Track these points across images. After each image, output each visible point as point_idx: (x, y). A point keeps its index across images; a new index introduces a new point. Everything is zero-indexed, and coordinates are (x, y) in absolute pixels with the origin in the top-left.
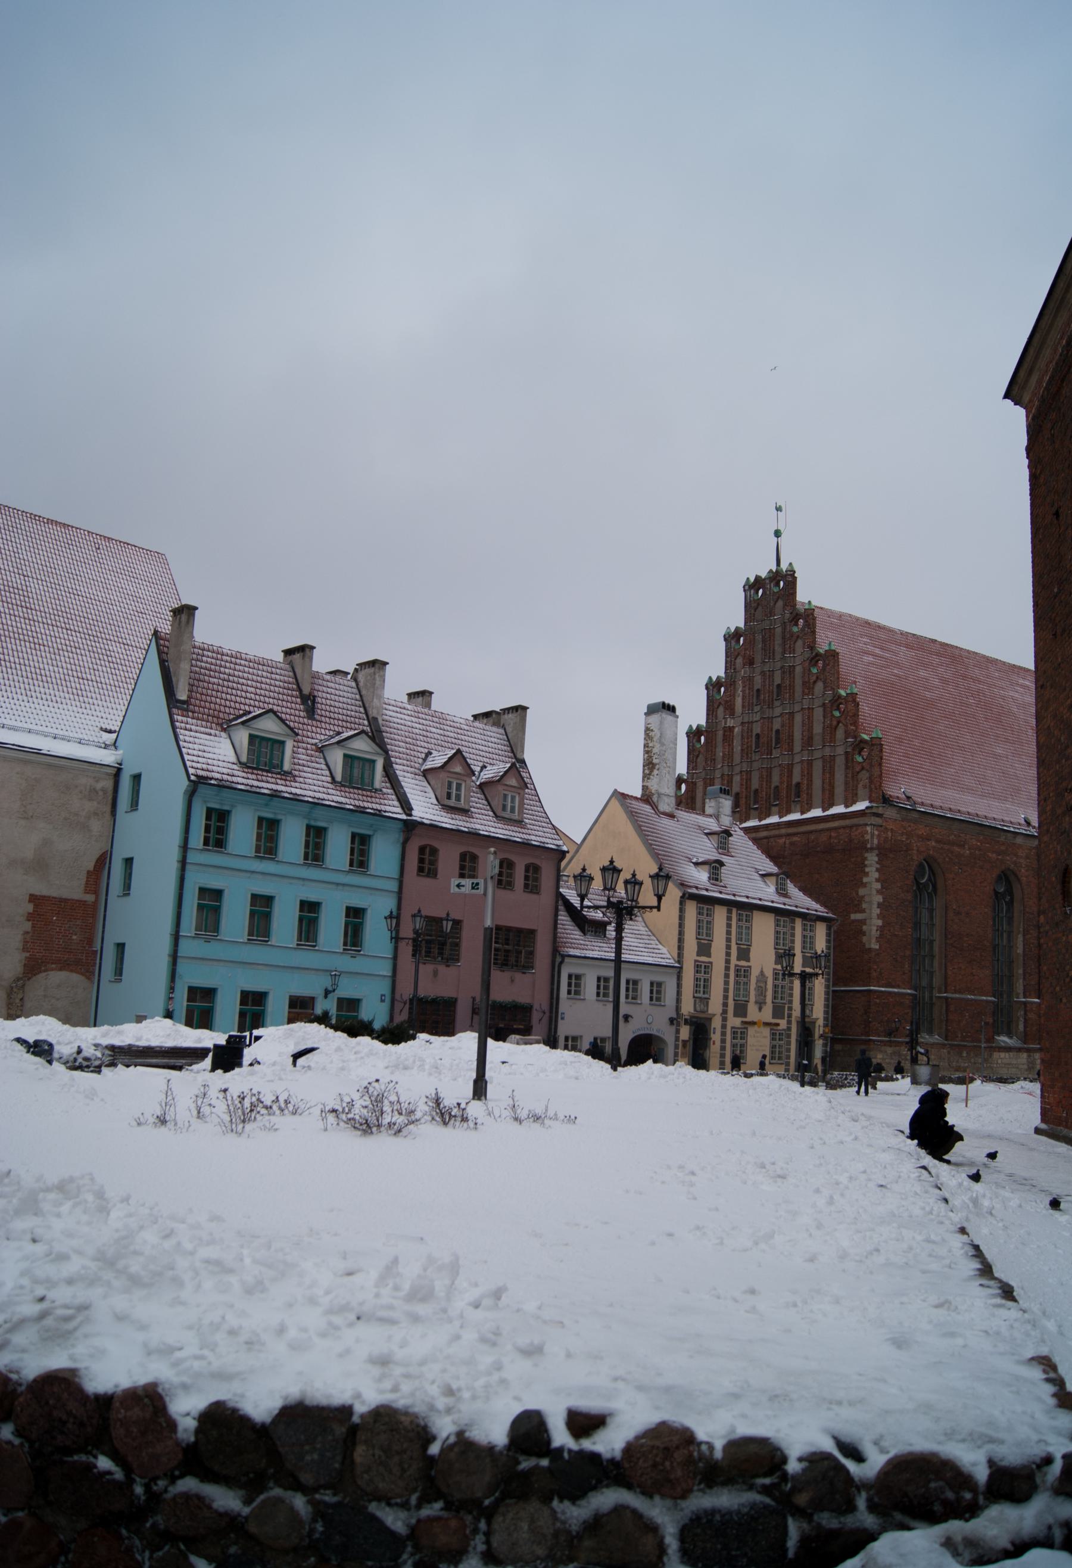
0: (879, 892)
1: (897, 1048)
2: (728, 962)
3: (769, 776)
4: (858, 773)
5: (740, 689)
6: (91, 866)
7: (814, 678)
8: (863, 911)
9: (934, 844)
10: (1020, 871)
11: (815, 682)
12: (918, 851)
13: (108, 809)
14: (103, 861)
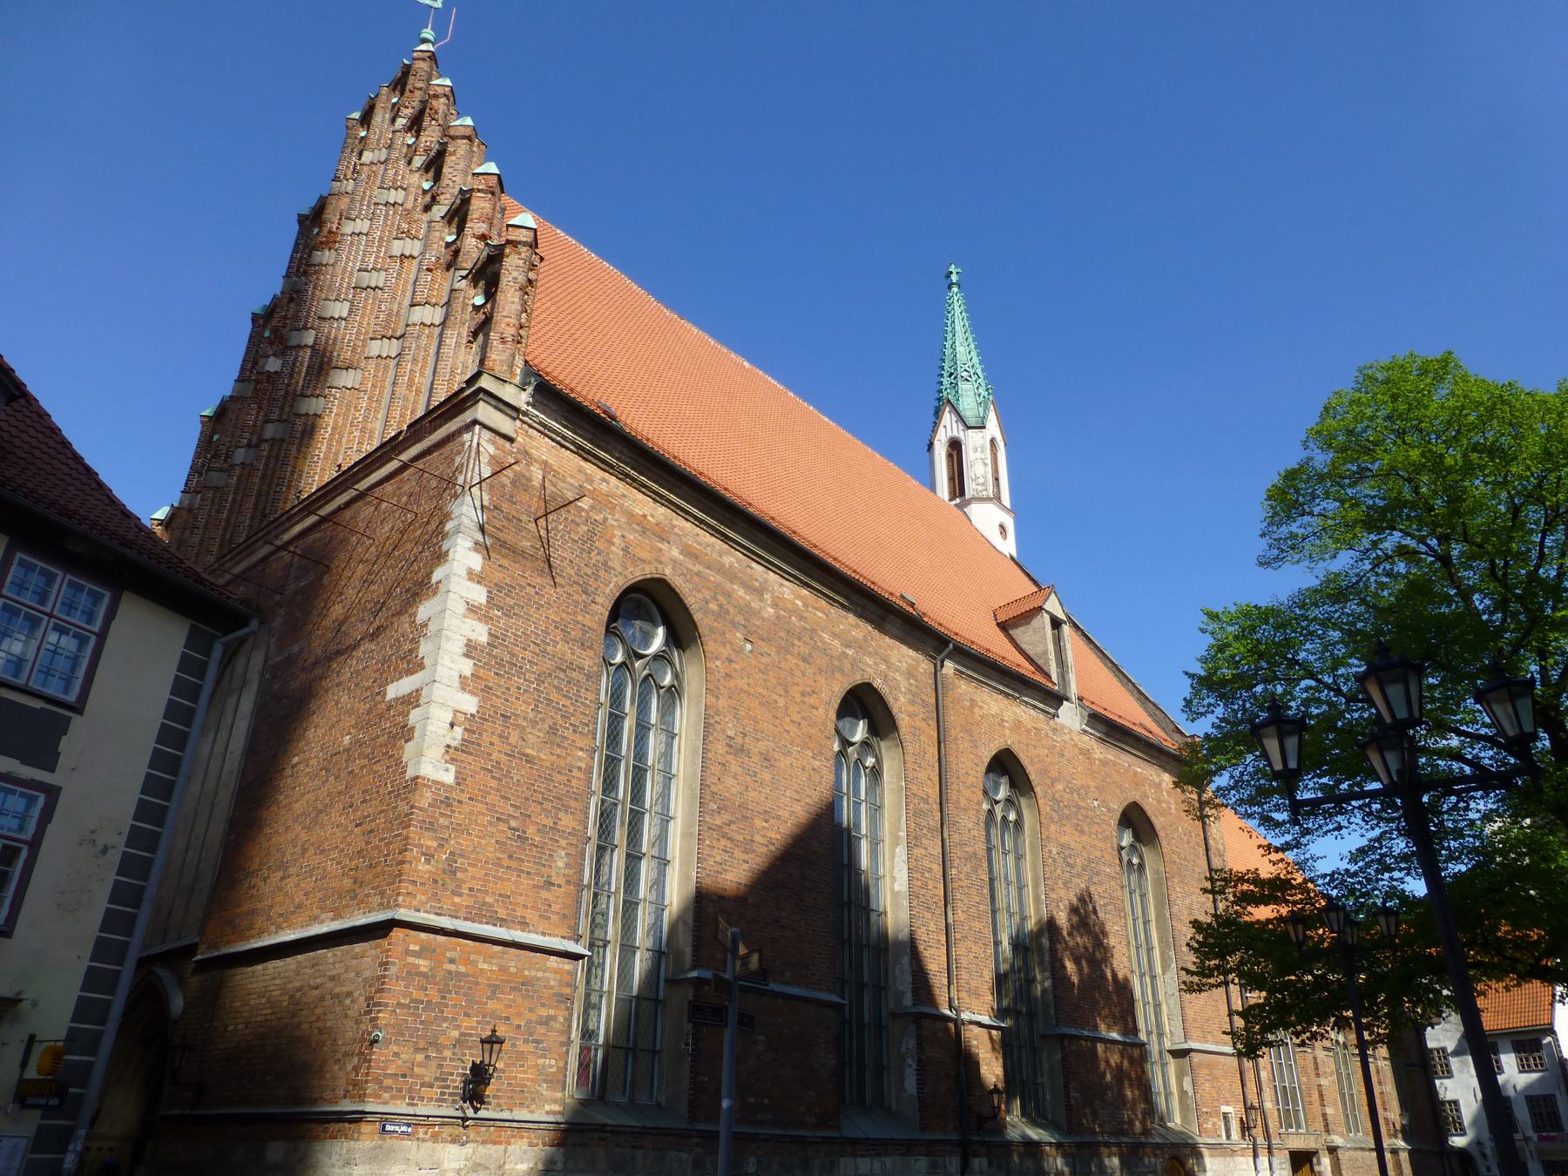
1: (493, 1150)
9: (675, 553)
12: (625, 550)
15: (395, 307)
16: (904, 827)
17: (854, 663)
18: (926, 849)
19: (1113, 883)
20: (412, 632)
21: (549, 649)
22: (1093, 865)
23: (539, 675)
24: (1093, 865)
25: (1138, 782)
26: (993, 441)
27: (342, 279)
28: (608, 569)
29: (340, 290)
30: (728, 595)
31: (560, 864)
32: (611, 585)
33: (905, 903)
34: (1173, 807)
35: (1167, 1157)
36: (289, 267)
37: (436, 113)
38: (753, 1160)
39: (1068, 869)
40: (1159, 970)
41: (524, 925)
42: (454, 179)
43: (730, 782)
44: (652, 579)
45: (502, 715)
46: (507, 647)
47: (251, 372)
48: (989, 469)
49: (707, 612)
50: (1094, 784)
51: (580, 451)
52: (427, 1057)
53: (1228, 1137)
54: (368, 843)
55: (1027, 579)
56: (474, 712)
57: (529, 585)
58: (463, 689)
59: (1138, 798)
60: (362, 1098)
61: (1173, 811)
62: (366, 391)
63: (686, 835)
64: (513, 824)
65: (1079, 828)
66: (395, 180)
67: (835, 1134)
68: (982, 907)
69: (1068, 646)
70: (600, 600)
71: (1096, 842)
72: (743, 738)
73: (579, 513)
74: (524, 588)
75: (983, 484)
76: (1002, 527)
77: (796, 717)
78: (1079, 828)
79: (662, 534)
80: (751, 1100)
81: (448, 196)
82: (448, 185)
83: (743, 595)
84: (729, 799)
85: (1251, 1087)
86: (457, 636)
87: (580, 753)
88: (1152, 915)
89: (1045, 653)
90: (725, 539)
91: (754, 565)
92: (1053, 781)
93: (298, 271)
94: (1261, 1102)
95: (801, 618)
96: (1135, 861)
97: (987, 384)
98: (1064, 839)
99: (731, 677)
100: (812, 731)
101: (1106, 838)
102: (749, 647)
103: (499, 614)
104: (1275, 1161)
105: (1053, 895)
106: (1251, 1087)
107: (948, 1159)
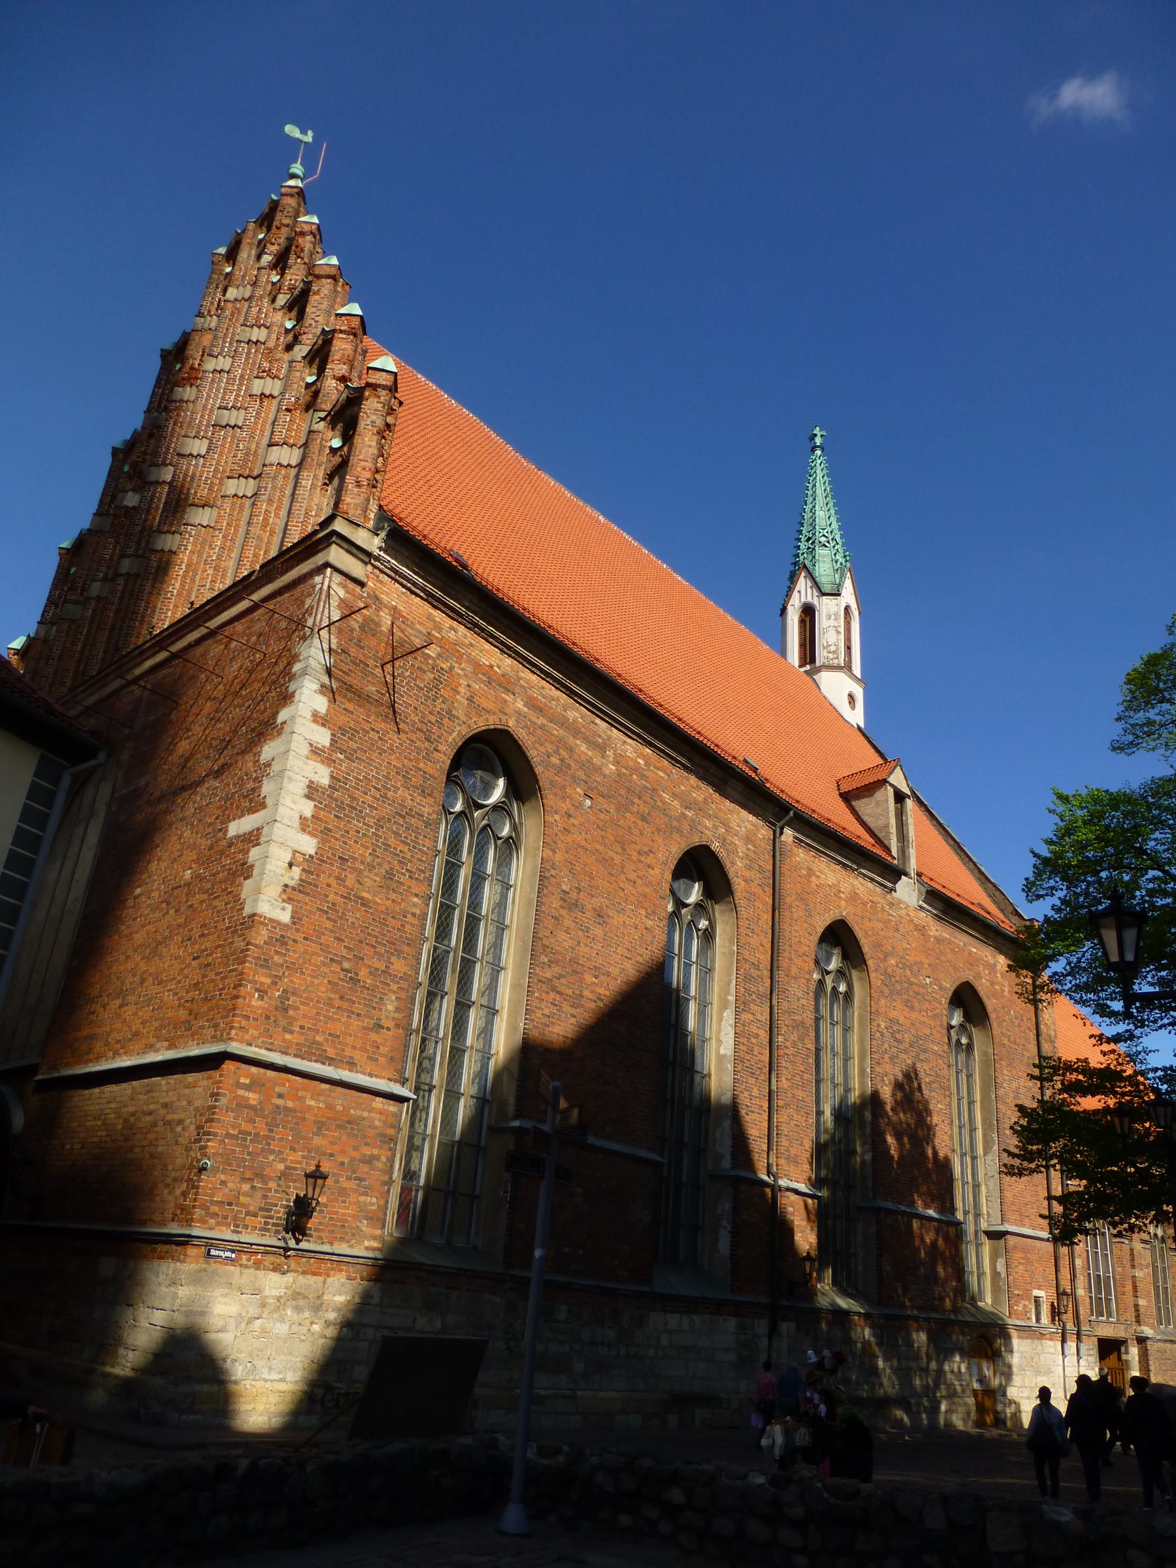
1: (312, 1280)
9: (520, 704)
10: (733, 864)
12: (470, 700)
15: (253, 447)
16: (733, 991)
17: (693, 824)
18: (754, 1014)
19: (940, 1061)
20: (256, 771)
21: (390, 794)
22: (921, 1042)
23: (378, 820)
24: (921, 1042)
25: (973, 961)
26: (847, 609)
27: (202, 416)
28: (452, 717)
29: (199, 427)
30: (571, 750)
31: (390, 1007)
32: (455, 734)
33: (730, 1067)
34: (1006, 989)
35: (975, 1335)
36: (151, 402)
37: (302, 250)
38: (564, 1308)
39: (896, 1044)
40: (980, 1150)
41: (351, 1065)
42: (317, 319)
43: (562, 936)
44: (495, 729)
45: (340, 858)
46: (347, 790)
47: (110, 506)
48: (842, 637)
49: (548, 765)
50: (927, 961)
51: (429, 598)
52: (253, 1187)
53: (1038, 1320)
54: (204, 976)
55: (873, 750)
56: (312, 852)
57: (373, 730)
58: (303, 830)
59: (971, 978)
60: (189, 1222)
61: (1006, 994)
62: (221, 529)
63: (516, 986)
64: (346, 965)
65: (909, 1004)
66: (258, 318)
67: (646, 1289)
68: (806, 1076)
69: (911, 821)
70: (442, 748)
71: (925, 1019)
72: (578, 893)
73: (426, 660)
74: (368, 732)
75: (834, 652)
76: (851, 697)
77: (632, 876)
78: (909, 1004)
79: (507, 685)
80: (566, 1250)
81: (310, 336)
82: (310, 325)
83: (586, 751)
84: (559, 953)
85: (1065, 1273)
86: (299, 777)
87: (415, 900)
88: (978, 1096)
89: (887, 826)
90: (571, 693)
91: (598, 721)
92: (886, 956)
93: (159, 405)
94: (1073, 1288)
95: (643, 777)
96: (964, 1041)
97: (845, 551)
98: (893, 1014)
99: (569, 832)
100: (647, 890)
101: (936, 1016)
102: (588, 802)
103: (342, 757)
104: (1083, 1347)
105: (878, 1069)
106: (1065, 1273)
107: (756, 1321)
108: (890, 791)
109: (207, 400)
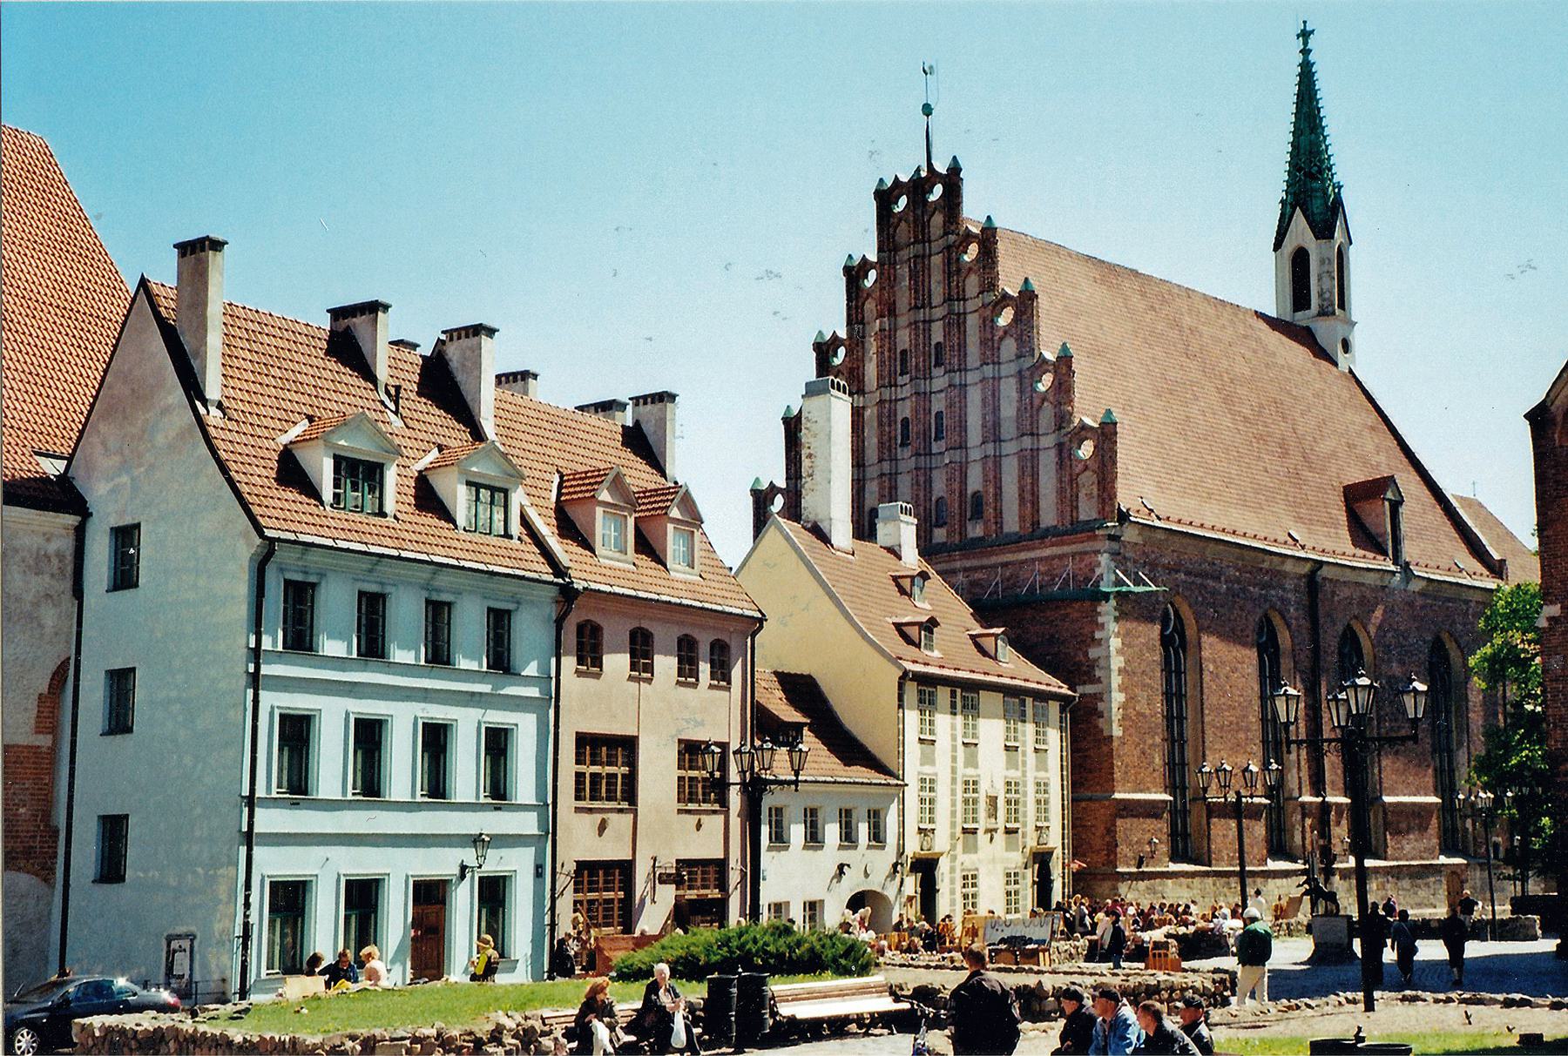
0: (1120, 652)
2: (954, 770)
3: (929, 481)
4: (1078, 475)
5: (874, 349)
6: (44, 687)
7: (1001, 333)
8: (1099, 681)
9: (1183, 576)
11: (1001, 339)
13: (68, 584)
14: (64, 676)
27: (924, 361)
31: (1157, 760)
108: (1387, 503)
109: (924, 348)
